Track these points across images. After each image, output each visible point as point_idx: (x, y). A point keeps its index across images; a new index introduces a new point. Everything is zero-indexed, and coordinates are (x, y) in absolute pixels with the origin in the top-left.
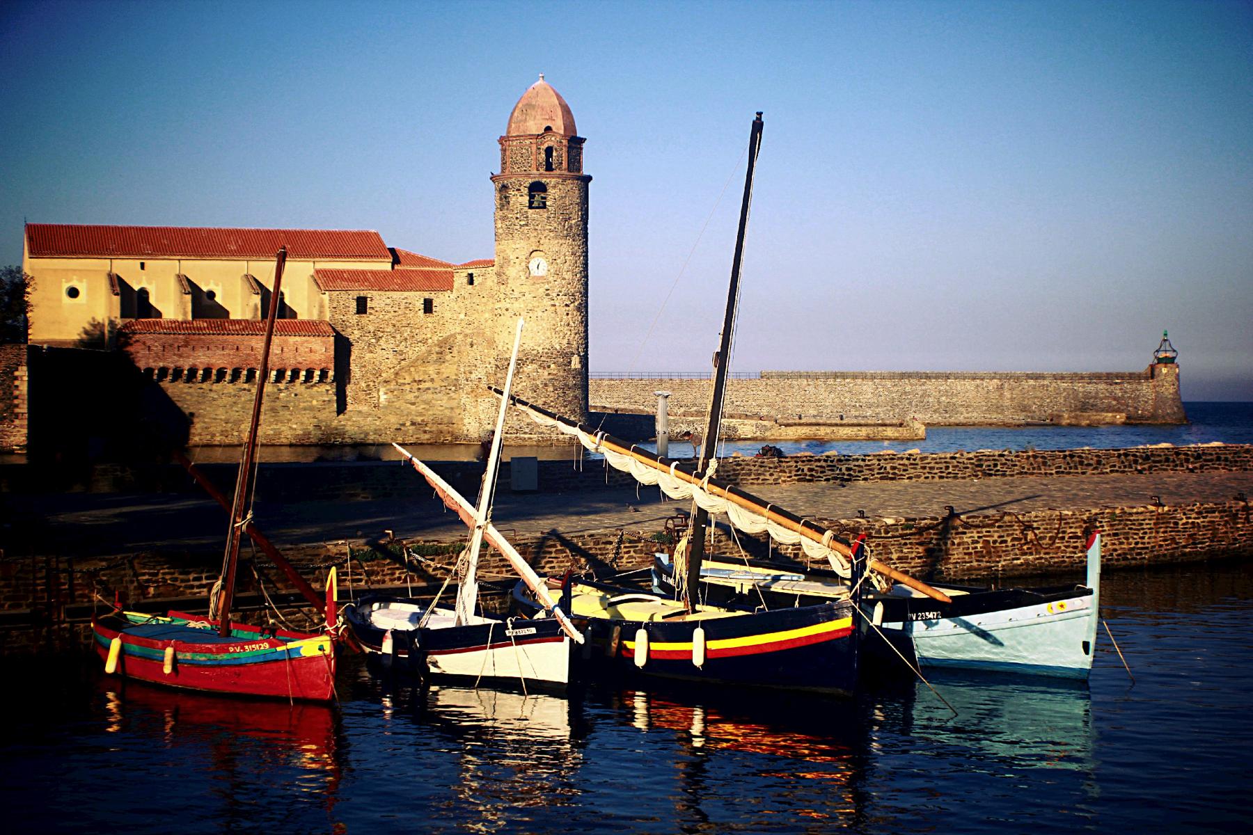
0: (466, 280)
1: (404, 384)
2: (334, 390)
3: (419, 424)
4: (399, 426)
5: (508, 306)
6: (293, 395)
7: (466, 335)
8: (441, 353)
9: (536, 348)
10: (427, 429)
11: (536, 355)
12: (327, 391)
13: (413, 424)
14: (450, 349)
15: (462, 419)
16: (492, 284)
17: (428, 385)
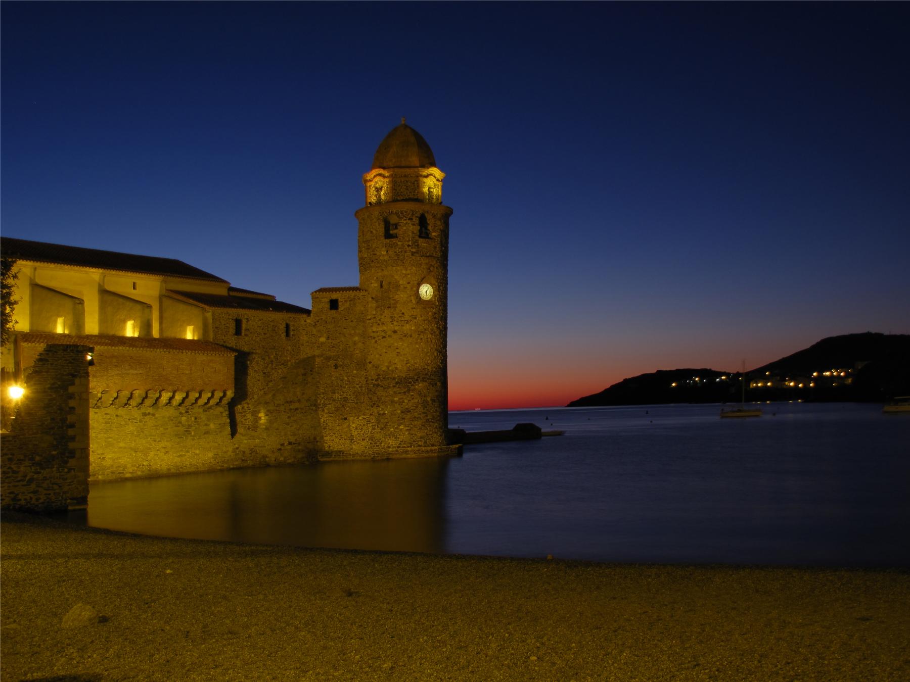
0: (328, 306)
1: (279, 405)
2: (227, 413)
3: (294, 444)
4: (279, 447)
5: (397, 328)
6: (193, 419)
7: (328, 358)
8: (305, 375)
9: (426, 367)
10: (300, 447)
11: (426, 374)
12: (221, 413)
13: (290, 443)
14: (311, 371)
15: (322, 437)
16: (362, 309)
17: (297, 405)
